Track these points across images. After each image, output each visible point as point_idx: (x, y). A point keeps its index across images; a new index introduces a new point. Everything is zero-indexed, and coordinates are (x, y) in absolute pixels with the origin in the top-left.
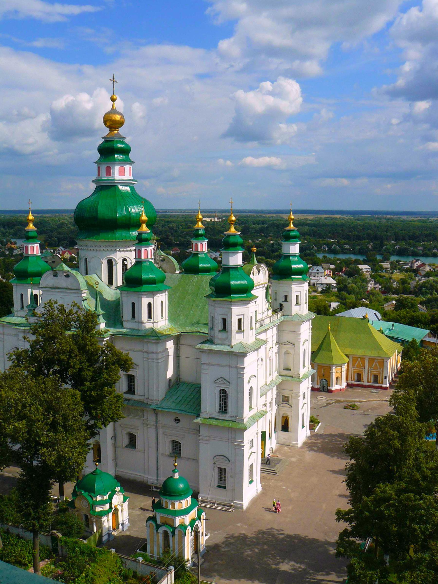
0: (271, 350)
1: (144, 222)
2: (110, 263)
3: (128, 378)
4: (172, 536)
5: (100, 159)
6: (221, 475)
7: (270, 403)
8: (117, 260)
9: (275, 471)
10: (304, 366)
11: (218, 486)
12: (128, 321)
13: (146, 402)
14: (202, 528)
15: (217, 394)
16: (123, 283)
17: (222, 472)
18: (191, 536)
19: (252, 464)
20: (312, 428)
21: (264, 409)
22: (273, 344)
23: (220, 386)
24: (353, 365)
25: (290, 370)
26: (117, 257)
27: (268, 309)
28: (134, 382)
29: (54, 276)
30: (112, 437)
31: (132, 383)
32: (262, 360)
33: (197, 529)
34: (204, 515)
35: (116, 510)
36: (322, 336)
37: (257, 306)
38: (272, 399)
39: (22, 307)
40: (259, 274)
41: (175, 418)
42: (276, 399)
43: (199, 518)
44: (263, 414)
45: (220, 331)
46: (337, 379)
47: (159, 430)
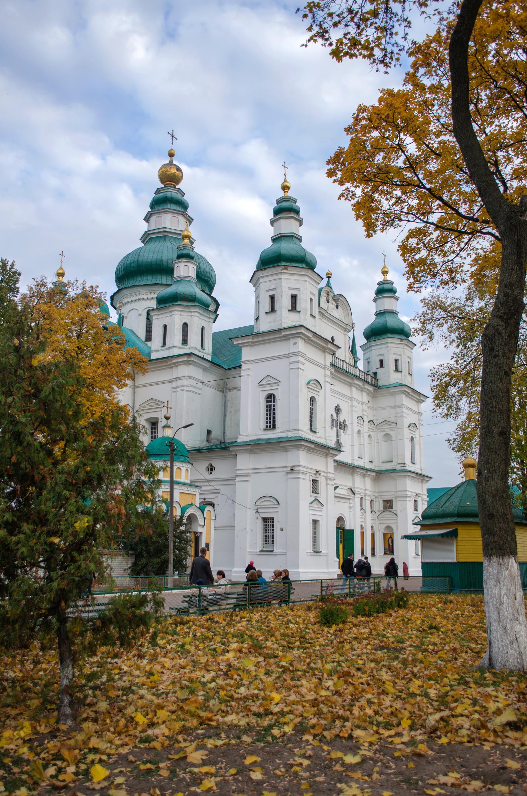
12: (156, 351)
17: (268, 522)
41: (206, 464)
45: (266, 313)
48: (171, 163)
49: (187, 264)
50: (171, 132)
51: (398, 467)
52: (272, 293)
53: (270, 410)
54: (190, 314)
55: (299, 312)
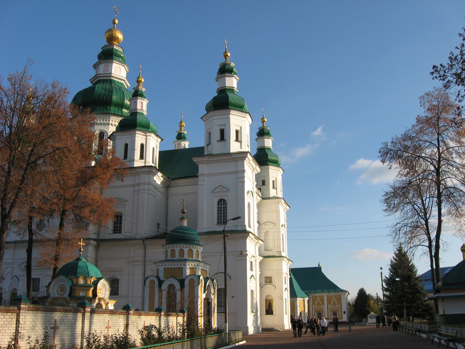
8: (108, 133)
15: (215, 205)
23: (217, 195)
24: (314, 304)
26: (108, 130)
28: (121, 223)
47: (146, 266)
49: (142, 101)
51: (276, 254)
52: (222, 127)
53: (221, 211)
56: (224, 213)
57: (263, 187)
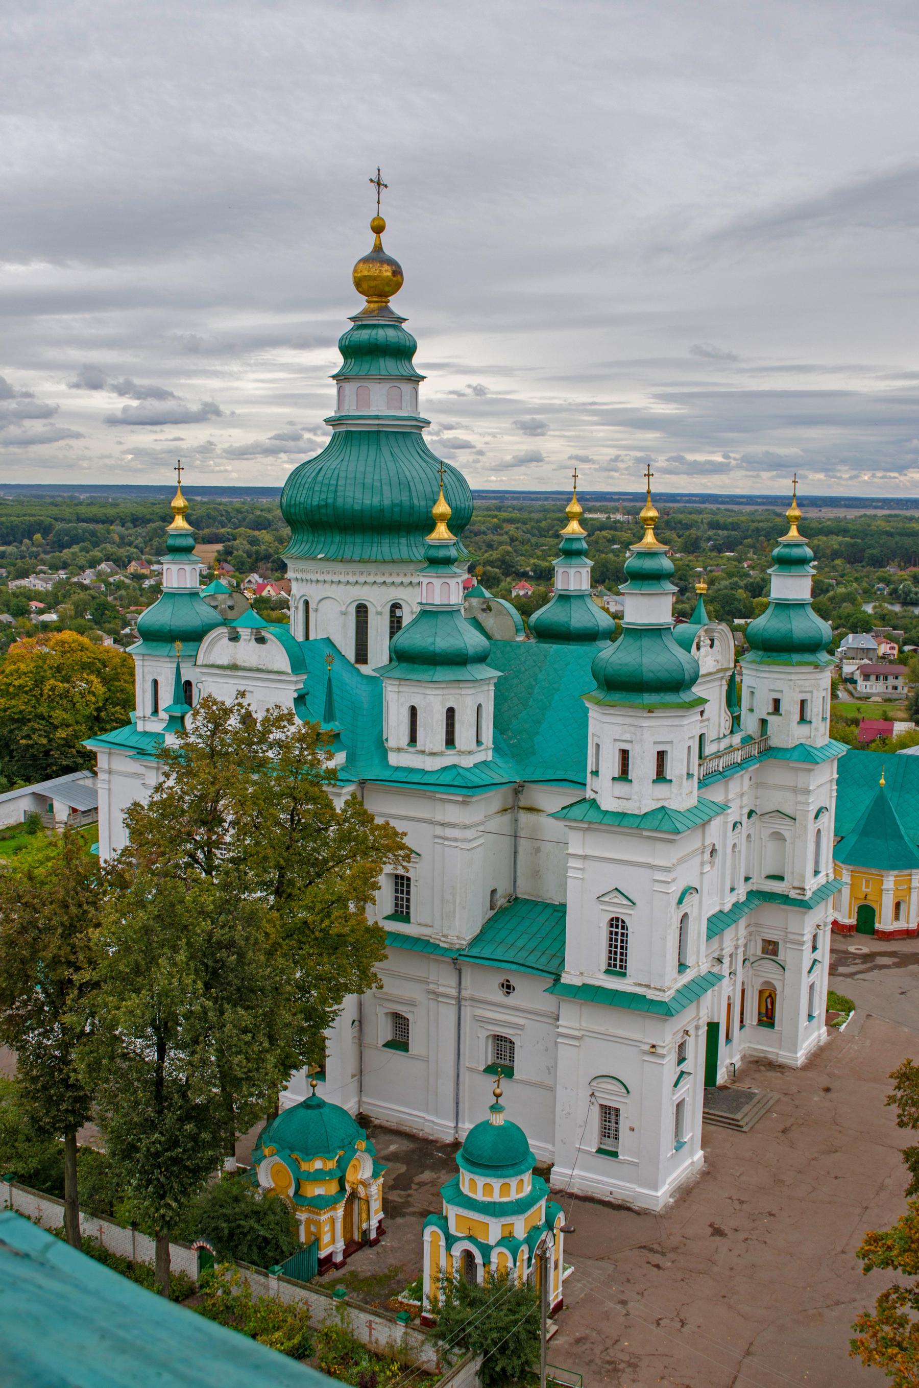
0: (737, 830)
1: (442, 517)
2: (362, 610)
3: (396, 884)
4: (484, 1265)
5: (344, 367)
6: (607, 1123)
7: (731, 956)
9: (738, 1121)
10: (816, 873)
11: (600, 1151)
12: (399, 750)
13: (437, 942)
14: (556, 1249)
16: (391, 660)
17: (610, 1115)
18: (529, 1267)
19: (684, 1099)
20: (832, 1023)
21: (715, 970)
22: (741, 815)
25: (781, 878)
27: (732, 732)
28: (408, 893)
29: (230, 640)
30: (354, 1021)
31: (405, 896)
32: (713, 852)
33: (544, 1252)
34: (561, 1220)
35: (354, 1195)
36: (866, 800)
37: (706, 723)
38: (737, 947)
39: (156, 711)
40: (712, 646)
41: (501, 980)
42: (745, 946)
43: (550, 1225)
44: (710, 981)
45: (614, 779)
46: (898, 905)
47: (463, 1008)
48: (378, 249)
50: (375, 178)
51: (793, 894)
53: (616, 940)
54: (458, 691)
55: (671, 781)
56: (622, 948)
57: (772, 720)
